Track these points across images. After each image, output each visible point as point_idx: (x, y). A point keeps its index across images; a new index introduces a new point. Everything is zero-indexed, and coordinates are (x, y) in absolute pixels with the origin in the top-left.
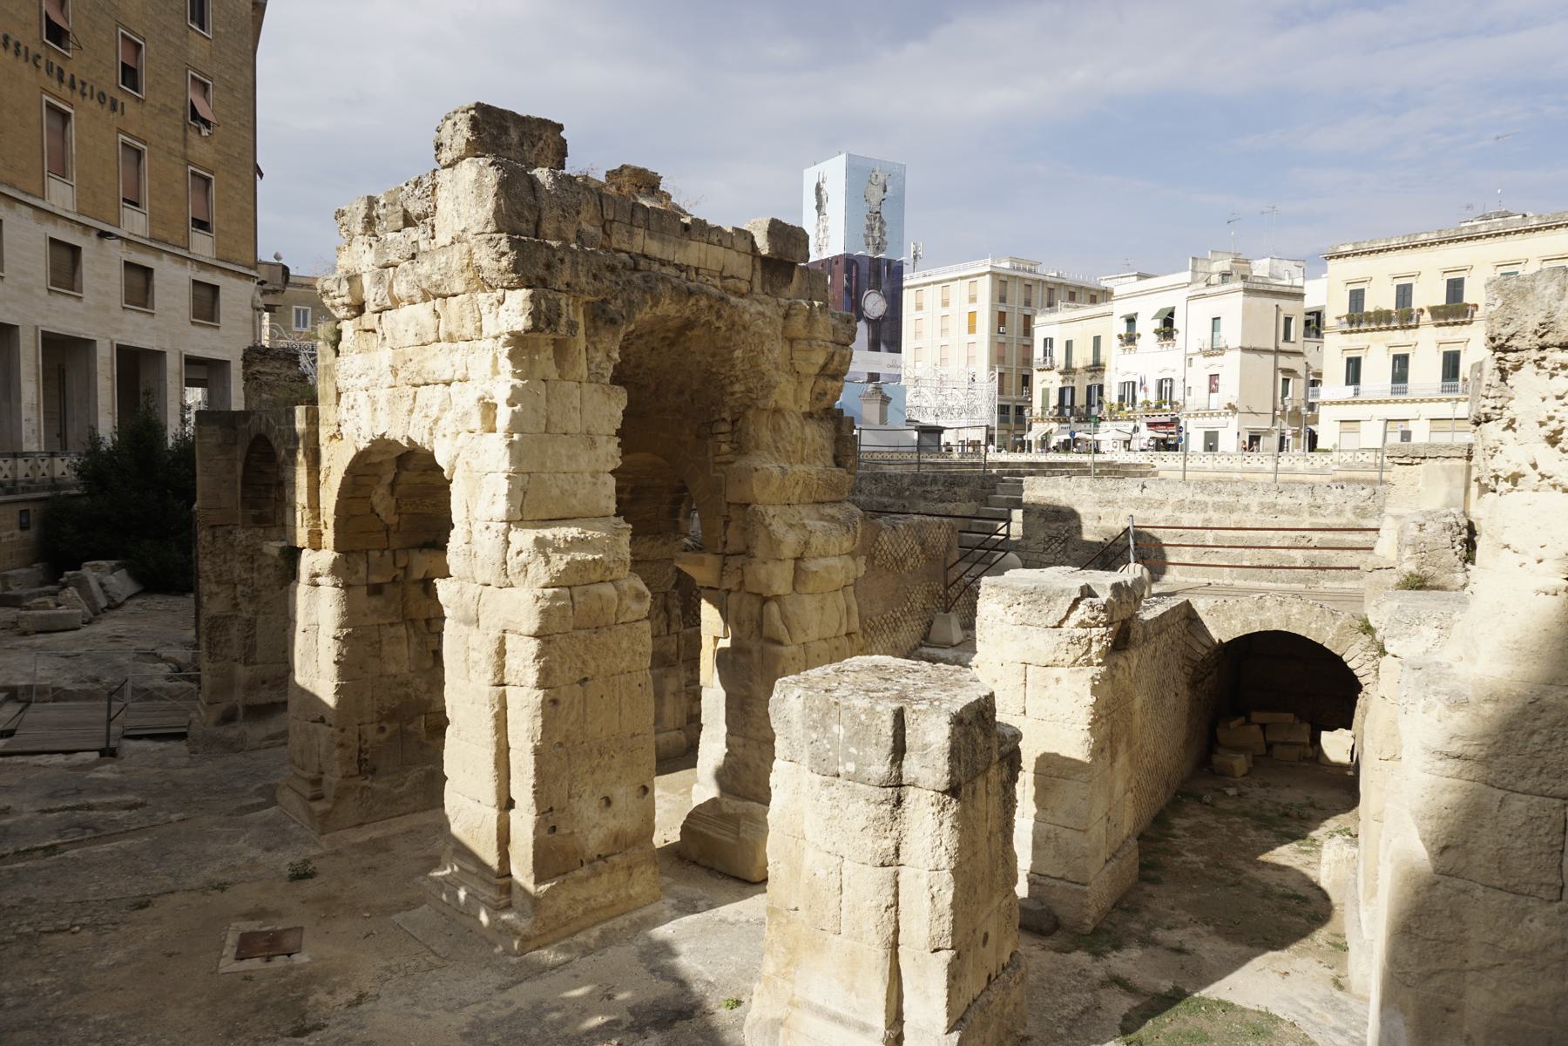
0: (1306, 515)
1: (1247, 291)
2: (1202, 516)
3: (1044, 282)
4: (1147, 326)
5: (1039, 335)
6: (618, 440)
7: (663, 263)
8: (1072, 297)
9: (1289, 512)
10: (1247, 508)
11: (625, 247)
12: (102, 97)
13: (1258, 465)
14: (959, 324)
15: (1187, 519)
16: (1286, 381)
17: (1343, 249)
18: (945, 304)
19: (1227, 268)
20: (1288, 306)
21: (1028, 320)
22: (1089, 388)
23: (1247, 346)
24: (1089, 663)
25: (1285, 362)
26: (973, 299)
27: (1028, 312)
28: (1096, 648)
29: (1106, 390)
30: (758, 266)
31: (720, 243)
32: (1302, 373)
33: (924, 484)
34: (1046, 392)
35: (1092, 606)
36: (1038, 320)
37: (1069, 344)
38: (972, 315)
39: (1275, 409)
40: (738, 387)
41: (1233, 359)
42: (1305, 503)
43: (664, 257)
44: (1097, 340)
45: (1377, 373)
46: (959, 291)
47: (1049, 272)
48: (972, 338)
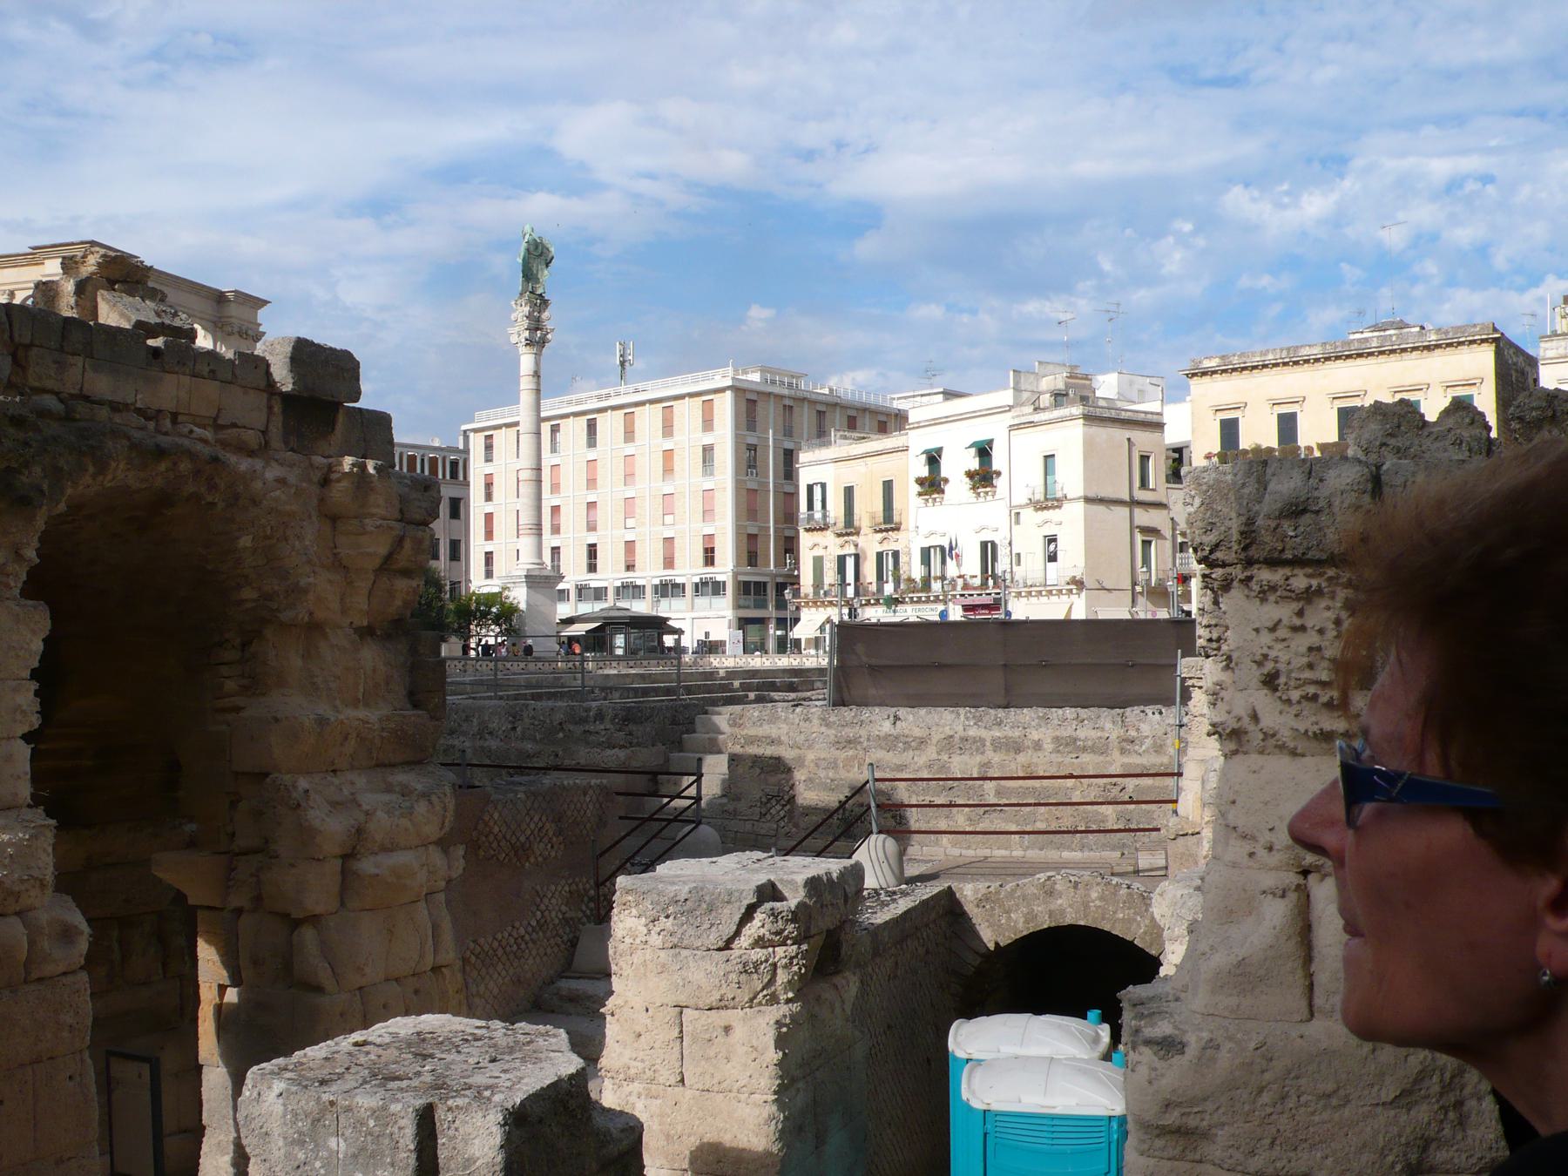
0: (1116, 754)
2: (979, 758)
3: (815, 402)
5: (806, 476)
6: (34, 686)
7: (116, 407)
8: (852, 424)
9: (1093, 749)
10: (1038, 746)
11: (50, 384)
15: (960, 764)
16: (1147, 544)
17: (1207, 364)
19: (1061, 385)
20: (1142, 439)
22: (880, 556)
23: (1091, 494)
24: (773, 1000)
25: (1144, 517)
27: (789, 445)
28: (782, 977)
29: (903, 559)
30: (277, 409)
31: (213, 375)
32: (1167, 533)
33: (583, 721)
34: (818, 563)
35: (774, 914)
36: (804, 457)
37: (849, 492)
39: (1134, 584)
40: (248, 594)
42: (1114, 736)
43: (118, 398)
44: (888, 486)
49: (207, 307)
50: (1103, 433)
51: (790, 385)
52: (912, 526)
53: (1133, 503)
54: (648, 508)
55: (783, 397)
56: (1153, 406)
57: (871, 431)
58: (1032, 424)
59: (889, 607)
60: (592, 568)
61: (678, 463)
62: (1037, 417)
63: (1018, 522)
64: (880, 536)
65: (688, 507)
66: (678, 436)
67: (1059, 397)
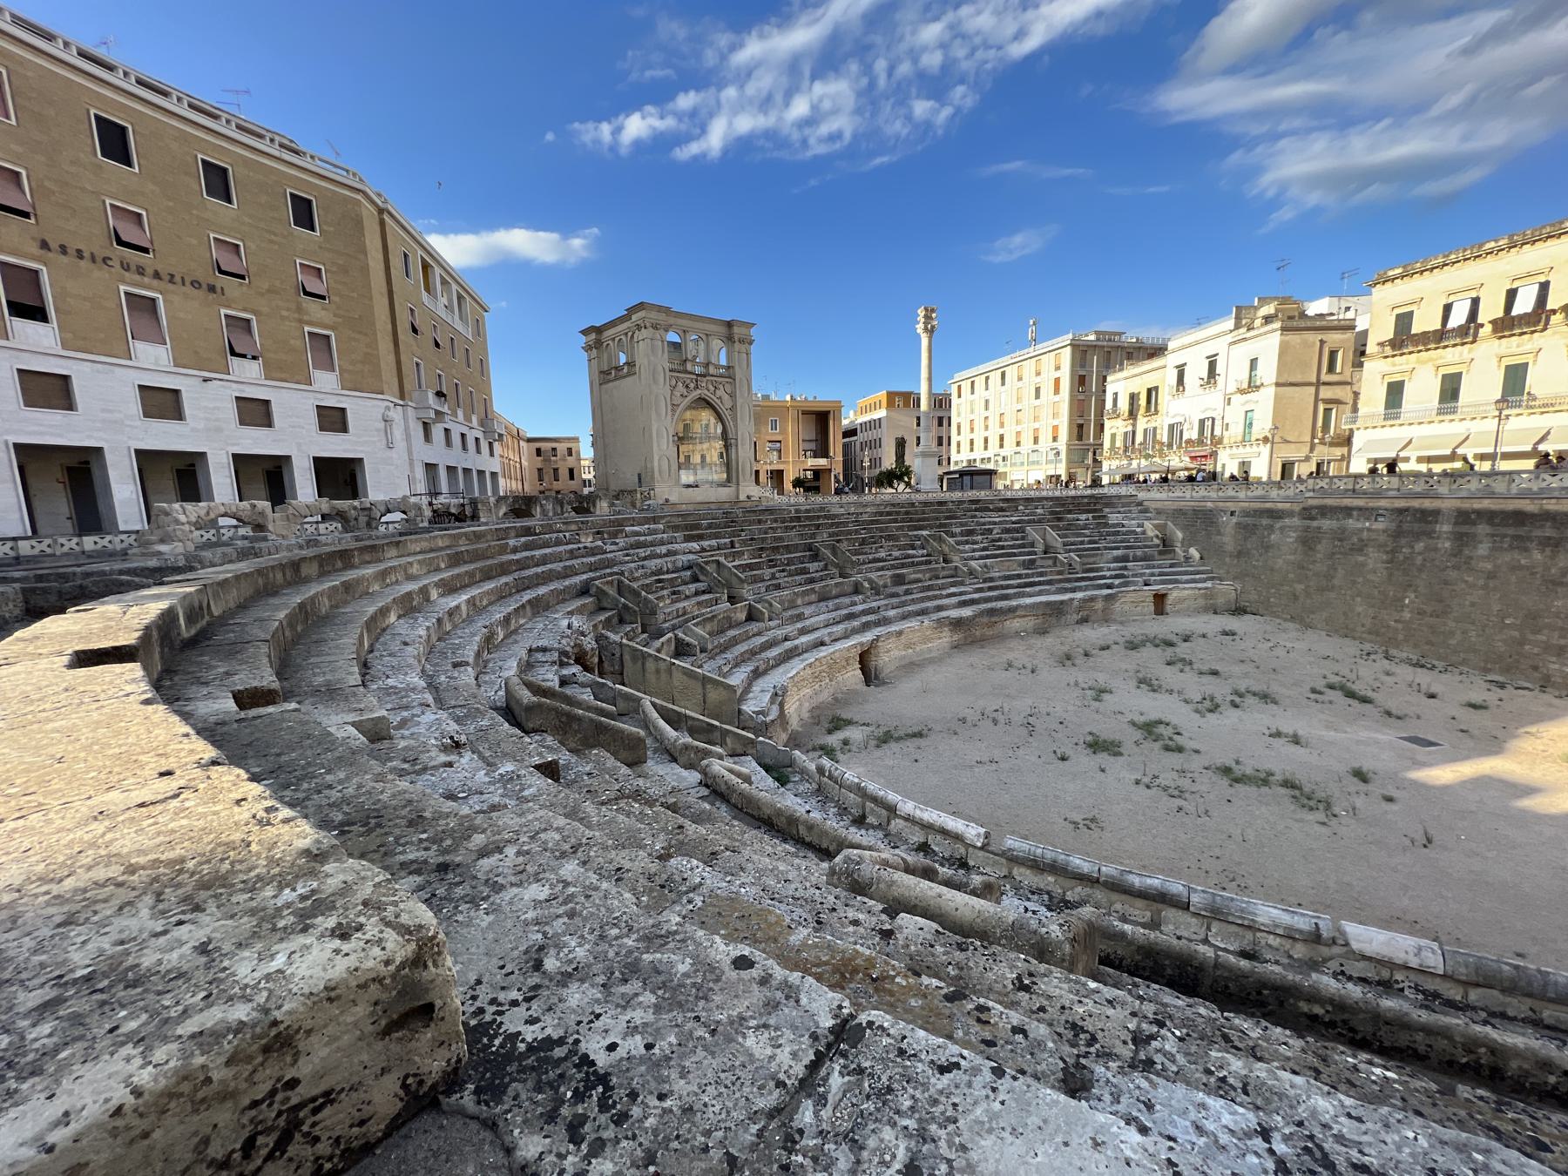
5: (1110, 389)
12: (196, 284)
13: (1233, 493)
14: (1047, 390)
16: (1327, 411)
19: (1272, 311)
20: (1334, 338)
25: (1325, 393)
26: (1058, 368)
34: (1113, 436)
38: (1057, 381)
39: (1313, 437)
41: (1267, 395)
45: (1423, 389)
46: (1048, 361)
47: (1130, 338)
48: (1057, 398)
50: (1294, 338)
53: (1319, 384)
54: (1026, 416)
56: (1350, 315)
58: (1245, 339)
60: (1001, 446)
61: (1042, 392)
62: (1252, 333)
65: (1045, 414)
67: (1268, 319)
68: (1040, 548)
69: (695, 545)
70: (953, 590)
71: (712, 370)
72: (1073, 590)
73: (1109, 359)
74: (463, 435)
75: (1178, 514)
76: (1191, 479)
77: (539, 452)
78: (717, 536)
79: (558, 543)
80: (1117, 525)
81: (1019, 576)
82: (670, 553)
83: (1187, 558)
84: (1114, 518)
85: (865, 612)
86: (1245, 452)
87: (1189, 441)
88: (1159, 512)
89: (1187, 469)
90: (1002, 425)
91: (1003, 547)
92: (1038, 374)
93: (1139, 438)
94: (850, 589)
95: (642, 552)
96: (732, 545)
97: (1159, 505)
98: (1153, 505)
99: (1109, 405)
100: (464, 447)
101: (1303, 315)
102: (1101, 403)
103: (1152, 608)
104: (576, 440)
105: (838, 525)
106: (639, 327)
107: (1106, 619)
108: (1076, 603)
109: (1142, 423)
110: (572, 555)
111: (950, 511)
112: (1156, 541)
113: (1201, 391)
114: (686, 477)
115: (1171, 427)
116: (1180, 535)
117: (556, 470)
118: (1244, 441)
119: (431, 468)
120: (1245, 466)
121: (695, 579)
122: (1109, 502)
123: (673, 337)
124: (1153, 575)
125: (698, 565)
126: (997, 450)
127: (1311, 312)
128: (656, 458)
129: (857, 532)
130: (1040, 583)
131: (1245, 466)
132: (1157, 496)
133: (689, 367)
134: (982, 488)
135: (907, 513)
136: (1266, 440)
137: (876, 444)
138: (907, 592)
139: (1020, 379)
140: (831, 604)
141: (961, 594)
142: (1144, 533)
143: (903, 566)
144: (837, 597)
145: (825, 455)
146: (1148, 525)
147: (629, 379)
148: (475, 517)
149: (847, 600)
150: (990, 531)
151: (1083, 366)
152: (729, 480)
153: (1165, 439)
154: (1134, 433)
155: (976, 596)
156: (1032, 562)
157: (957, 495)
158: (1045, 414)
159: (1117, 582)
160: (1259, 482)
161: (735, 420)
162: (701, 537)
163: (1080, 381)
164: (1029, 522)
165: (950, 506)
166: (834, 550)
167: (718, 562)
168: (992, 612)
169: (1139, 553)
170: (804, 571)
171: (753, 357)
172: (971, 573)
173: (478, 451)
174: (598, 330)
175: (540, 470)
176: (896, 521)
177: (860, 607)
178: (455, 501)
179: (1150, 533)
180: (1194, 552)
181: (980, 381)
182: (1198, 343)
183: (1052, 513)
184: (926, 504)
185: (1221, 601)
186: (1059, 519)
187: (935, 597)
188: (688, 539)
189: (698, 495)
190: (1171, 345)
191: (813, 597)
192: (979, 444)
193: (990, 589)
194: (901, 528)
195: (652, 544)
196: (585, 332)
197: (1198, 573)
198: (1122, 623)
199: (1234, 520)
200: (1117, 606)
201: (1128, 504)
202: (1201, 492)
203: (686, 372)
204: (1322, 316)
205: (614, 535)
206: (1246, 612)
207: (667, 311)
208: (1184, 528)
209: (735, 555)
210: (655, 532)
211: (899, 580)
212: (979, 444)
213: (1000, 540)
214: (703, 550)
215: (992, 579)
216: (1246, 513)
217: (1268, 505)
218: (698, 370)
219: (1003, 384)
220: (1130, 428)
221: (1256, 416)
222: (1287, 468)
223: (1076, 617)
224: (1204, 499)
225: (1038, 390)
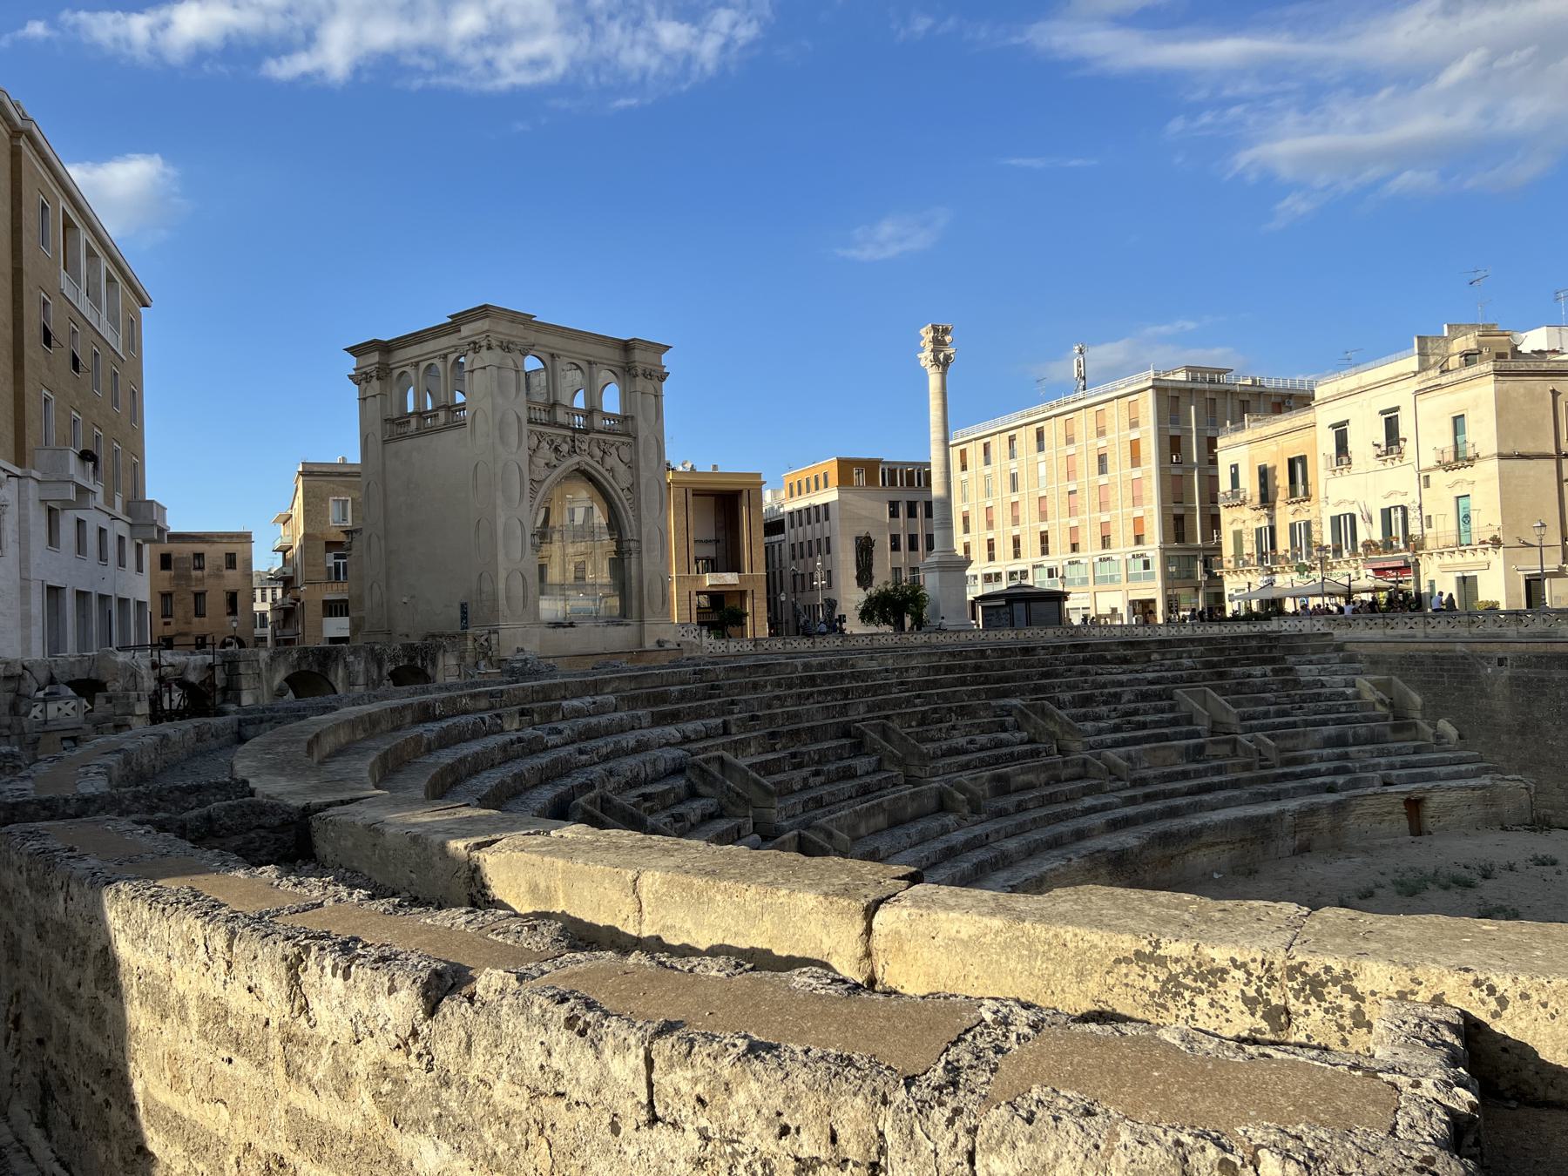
1: (1499, 373)
3: (1234, 393)
4: (1366, 435)
5: (1224, 460)
18: (1101, 433)
19: (1473, 346)
21: (1212, 443)
22: (1292, 526)
23: (1505, 452)
26: (1134, 424)
27: (1210, 434)
29: (1314, 528)
34: (1238, 536)
36: (1220, 442)
38: (1135, 445)
46: (1116, 414)
48: (1137, 473)
49: (616, 355)
51: (1212, 381)
52: (1322, 495)
54: (1087, 500)
55: (1204, 391)
57: (1266, 413)
58: (1439, 386)
59: (1301, 574)
60: (1045, 551)
63: (1427, 485)
64: (1291, 508)
65: (1119, 497)
66: (1109, 436)
67: (1469, 358)
68: (1203, 727)
69: (672, 732)
70: (1088, 801)
71: (599, 423)
72: (1277, 797)
73: (1214, 411)
74: (102, 531)
75: (1408, 664)
76: (1373, 605)
77: (166, 561)
78: (698, 714)
79: (476, 734)
80: (1315, 683)
81: (1185, 775)
82: (642, 747)
83: (1439, 737)
84: (1306, 672)
85: (971, 845)
86: (1466, 562)
87: (1369, 545)
88: (1375, 662)
89: (1377, 589)
90: (1043, 516)
91: (1144, 726)
92: (1101, 433)
93: (1283, 543)
94: (931, 803)
95: (604, 745)
96: (726, 730)
97: (1372, 649)
98: (1363, 650)
99: (1225, 484)
100: (102, 557)
101: (1516, 353)
102: (1211, 482)
103: (1405, 823)
104: (246, 538)
105: (875, 690)
106: (476, 347)
107: (1339, 847)
108: (1288, 819)
109: (1285, 515)
110: (508, 754)
111: (1043, 663)
112: (1381, 710)
113: (1378, 463)
114: (550, 608)
115: (1336, 521)
116: (1417, 699)
117: (199, 596)
118: (1461, 545)
119: (54, 592)
120: (1467, 584)
121: (693, 794)
122: (1292, 645)
123: (531, 363)
124: (1392, 767)
125: (694, 765)
126: (1038, 559)
127: (1525, 348)
128: (502, 575)
129: (908, 701)
130: (1221, 786)
131: (1467, 584)
132: (1365, 632)
133: (561, 416)
134: (1046, 624)
135: (977, 668)
136: (1496, 542)
137: (825, 546)
138: (1021, 808)
139: (1070, 441)
140: (914, 829)
141: (1105, 808)
142: (1358, 696)
143: (997, 761)
144: (915, 818)
145: (735, 567)
146: (1363, 683)
147: (452, 435)
148: (232, 690)
149: (934, 824)
150: (1117, 697)
151: (1175, 422)
152: (625, 612)
153: (1327, 540)
154: (1272, 529)
155: (1129, 811)
156: (1200, 749)
157: (1007, 636)
158: (1119, 497)
159: (1340, 780)
160: (1492, 608)
161: (637, 508)
162: (674, 717)
163: (1172, 446)
164: (1175, 680)
165: (1042, 654)
166: (885, 733)
167: (721, 759)
168: (1165, 838)
169: (1362, 729)
170: (848, 774)
171: (666, 402)
172: (1112, 770)
173: (122, 563)
174: (385, 348)
175: (166, 597)
176: (963, 682)
177: (958, 837)
178: (198, 659)
179: (1370, 696)
180: (1444, 725)
181: (999, 445)
182: (1363, 390)
183: (1208, 665)
184: (1003, 652)
185: (1507, 807)
186: (1221, 676)
187: (1066, 816)
188: (659, 720)
189: (572, 641)
190: (1320, 393)
191: (880, 820)
192: (1004, 548)
193: (1148, 798)
194: (975, 694)
195: (608, 731)
196: (355, 351)
197: (1460, 762)
198: (1366, 851)
199: (1507, 673)
200: (1351, 822)
201: (1322, 649)
202: (1441, 628)
203: (554, 424)
204: (1540, 352)
205: (547, 716)
206: (1550, 827)
207: (526, 320)
208: (1421, 688)
209: (739, 747)
210: (600, 710)
211: (1001, 786)
212: (1004, 548)
213: (1136, 712)
214: (686, 739)
215: (1143, 782)
216: (1524, 661)
217: (1559, 648)
218: (579, 421)
219: (1041, 448)
220: (1265, 523)
221: (1474, 503)
222: (1533, 586)
223: (1291, 843)
224: (1446, 639)
225: (1102, 459)
